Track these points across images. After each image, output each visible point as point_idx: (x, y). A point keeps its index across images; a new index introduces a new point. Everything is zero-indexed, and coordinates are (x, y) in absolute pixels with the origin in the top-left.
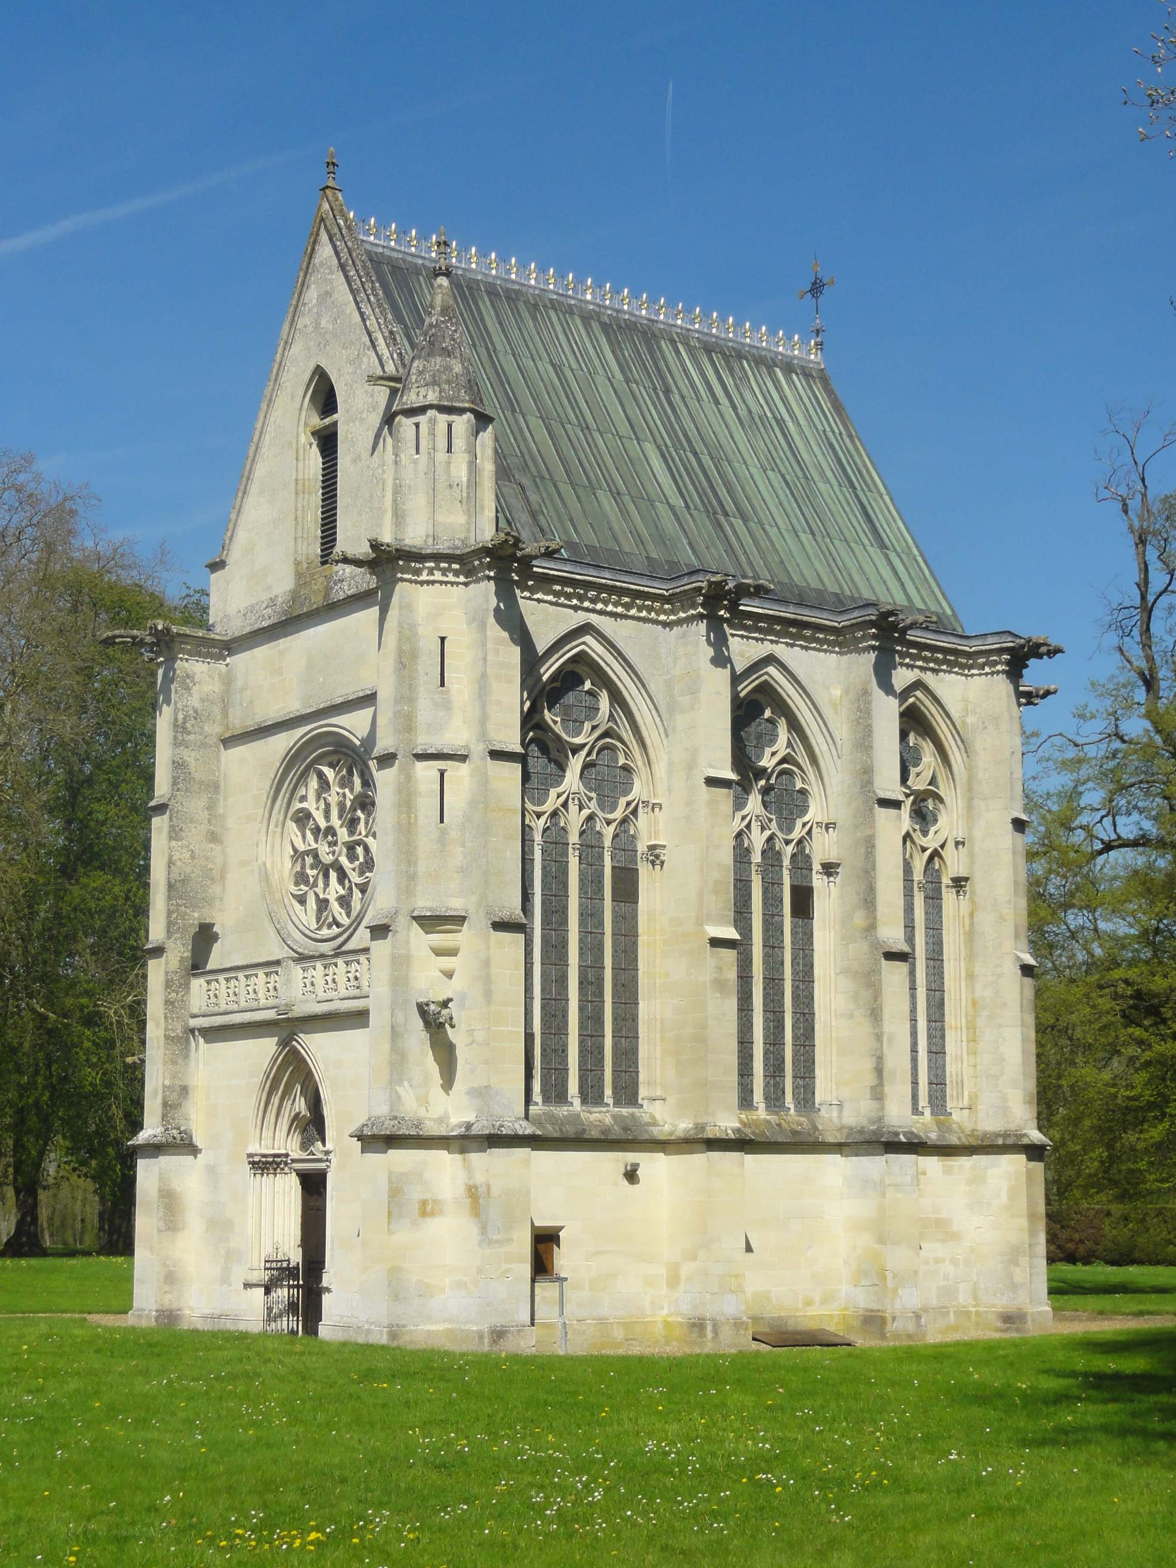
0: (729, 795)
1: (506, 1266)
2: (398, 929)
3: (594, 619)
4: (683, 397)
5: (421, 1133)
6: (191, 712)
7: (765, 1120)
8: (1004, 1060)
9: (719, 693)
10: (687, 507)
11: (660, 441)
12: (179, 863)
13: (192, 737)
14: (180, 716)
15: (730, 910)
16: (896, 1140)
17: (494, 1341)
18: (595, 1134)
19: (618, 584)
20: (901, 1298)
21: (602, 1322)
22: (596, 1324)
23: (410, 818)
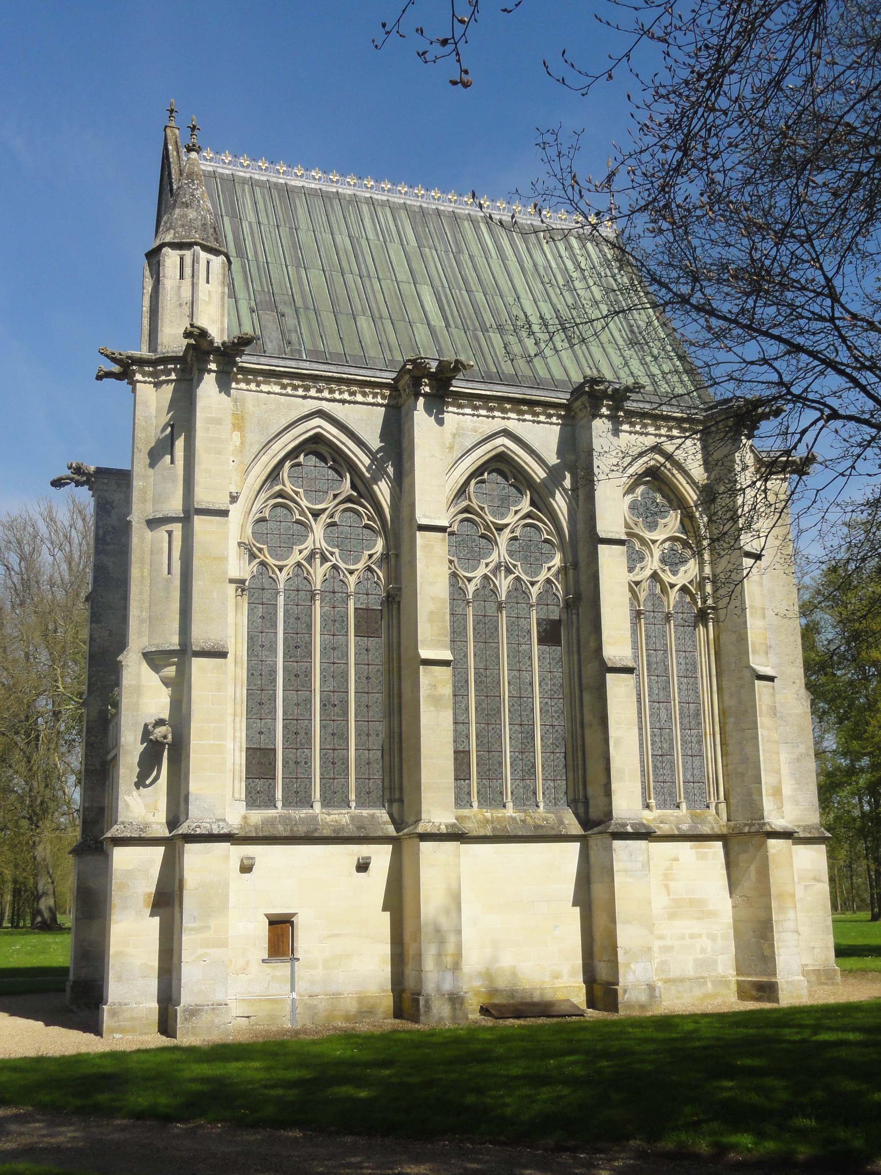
0: (443, 540)
1: (201, 951)
2: (129, 664)
3: (326, 406)
4: (471, 257)
5: (143, 835)
6: (110, 529)
7: (511, 816)
8: (748, 758)
9: (433, 456)
10: (448, 325)
11: (437, 283)
12: (98, 640)
13: (111, 547)
14: (101, 532)
15: (445, 636)
16: (622, 830)
17: (186, 1019)
18: (326, 832)
19: (344, 376)
20: (634, 972)
21: (336, 995)
22: (328, 999)
23: (143, 572)
